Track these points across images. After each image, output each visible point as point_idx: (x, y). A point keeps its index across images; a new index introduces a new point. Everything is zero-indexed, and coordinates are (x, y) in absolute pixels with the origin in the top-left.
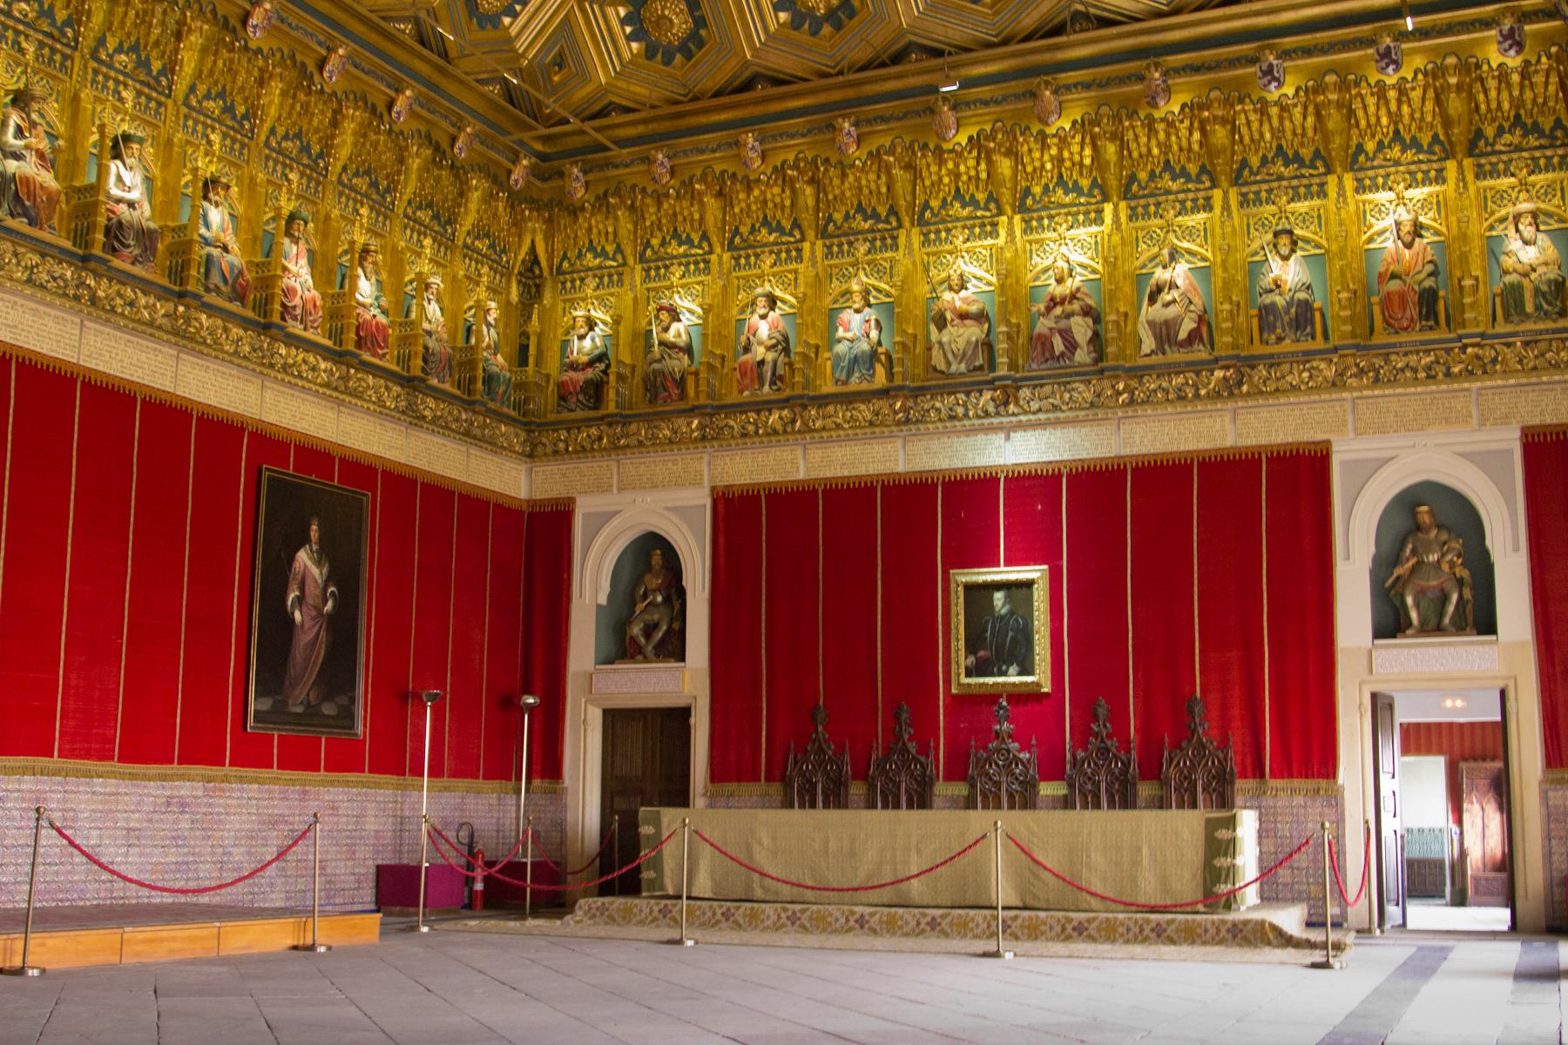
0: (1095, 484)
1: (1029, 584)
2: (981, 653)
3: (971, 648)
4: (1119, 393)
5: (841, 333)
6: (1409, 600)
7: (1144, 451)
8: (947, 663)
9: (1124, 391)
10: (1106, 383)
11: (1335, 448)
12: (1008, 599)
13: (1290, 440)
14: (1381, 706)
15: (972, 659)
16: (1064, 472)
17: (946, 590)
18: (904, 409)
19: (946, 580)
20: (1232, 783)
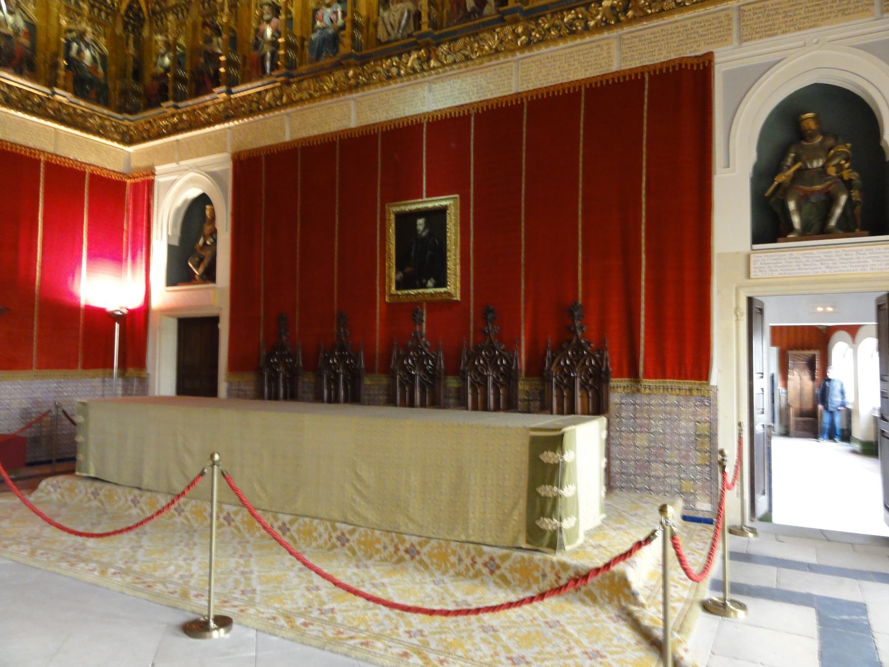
0: (496, 120)
1: (443, 211)
2: (408, 270)
3: (399, 267)
4: (518, 36)
5: (318, 23)
6: (792, 205)
7: (538, 85)
8: (383, 279)
9: (523, 34)
10: (508, 29)
11: (717, 59)
12: (427, 224)
13: (673, 57)
14: (754, 310)
15: (401, 274)
16: (473, 112)
17: (383, 220)
18: (356, 76)
19: (383, 212)
20: (607, 382)
